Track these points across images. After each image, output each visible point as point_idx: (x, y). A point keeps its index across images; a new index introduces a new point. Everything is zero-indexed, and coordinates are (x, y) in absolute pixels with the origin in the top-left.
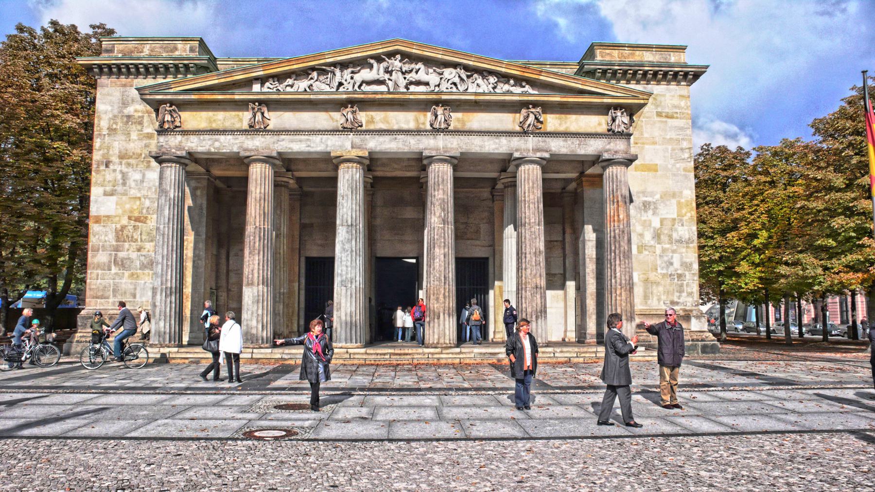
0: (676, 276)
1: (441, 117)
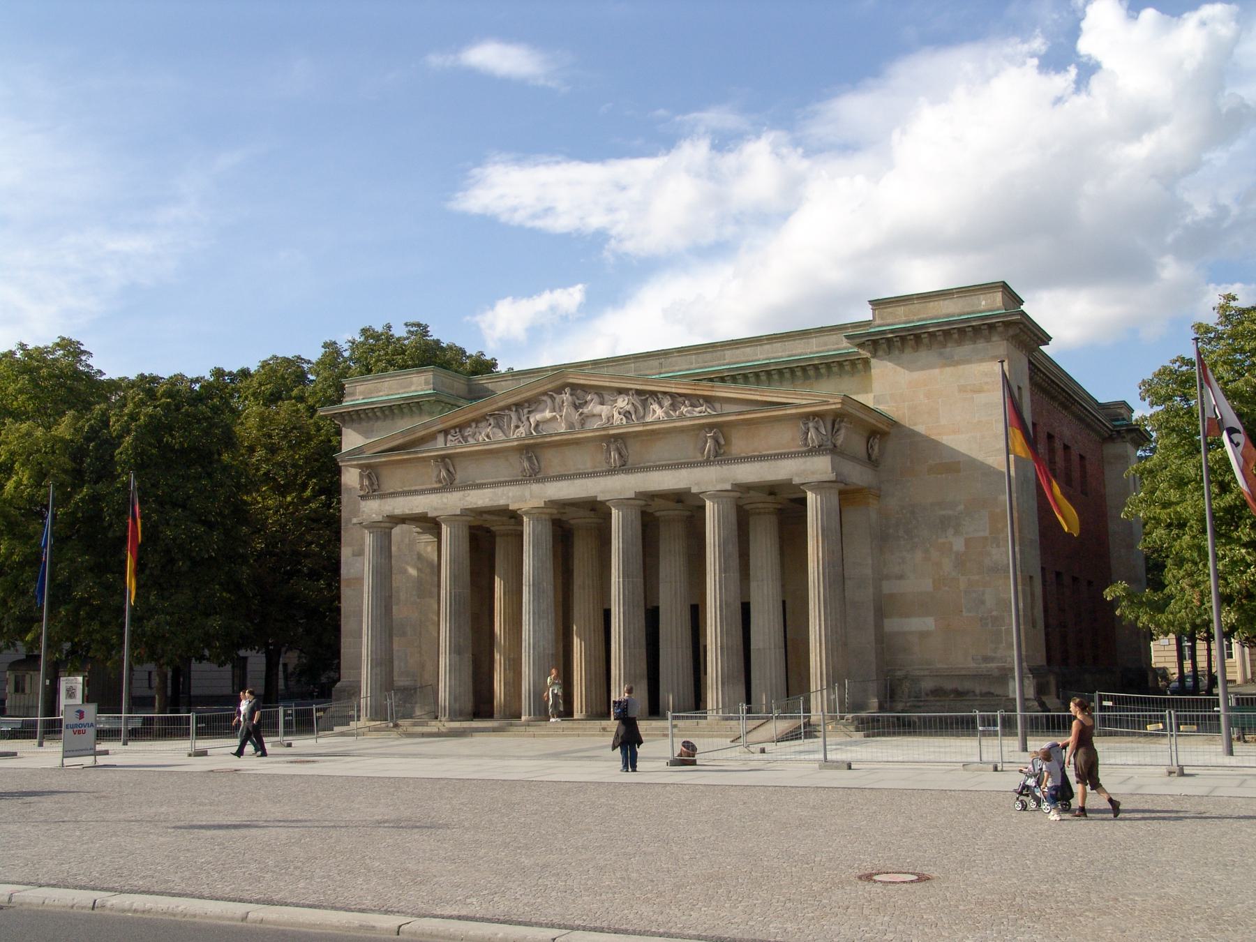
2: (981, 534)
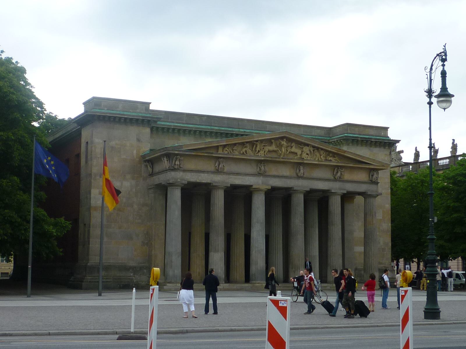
1: (302, 171)
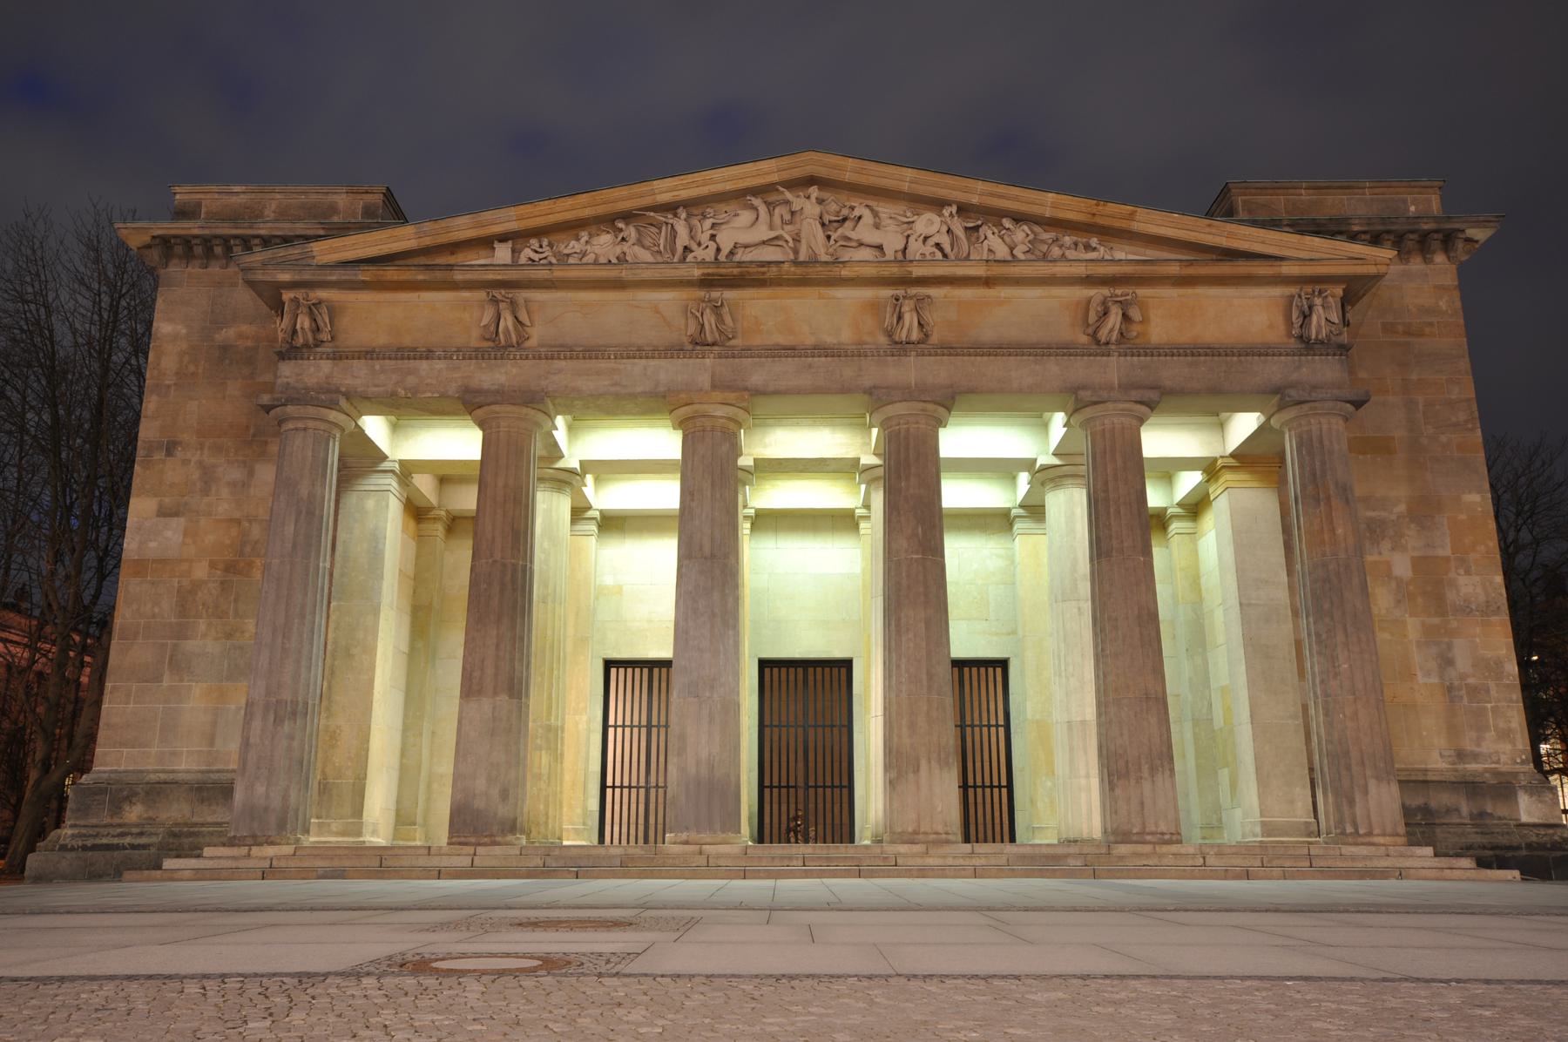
0: (1464, 692)
2: (1440, 552)
